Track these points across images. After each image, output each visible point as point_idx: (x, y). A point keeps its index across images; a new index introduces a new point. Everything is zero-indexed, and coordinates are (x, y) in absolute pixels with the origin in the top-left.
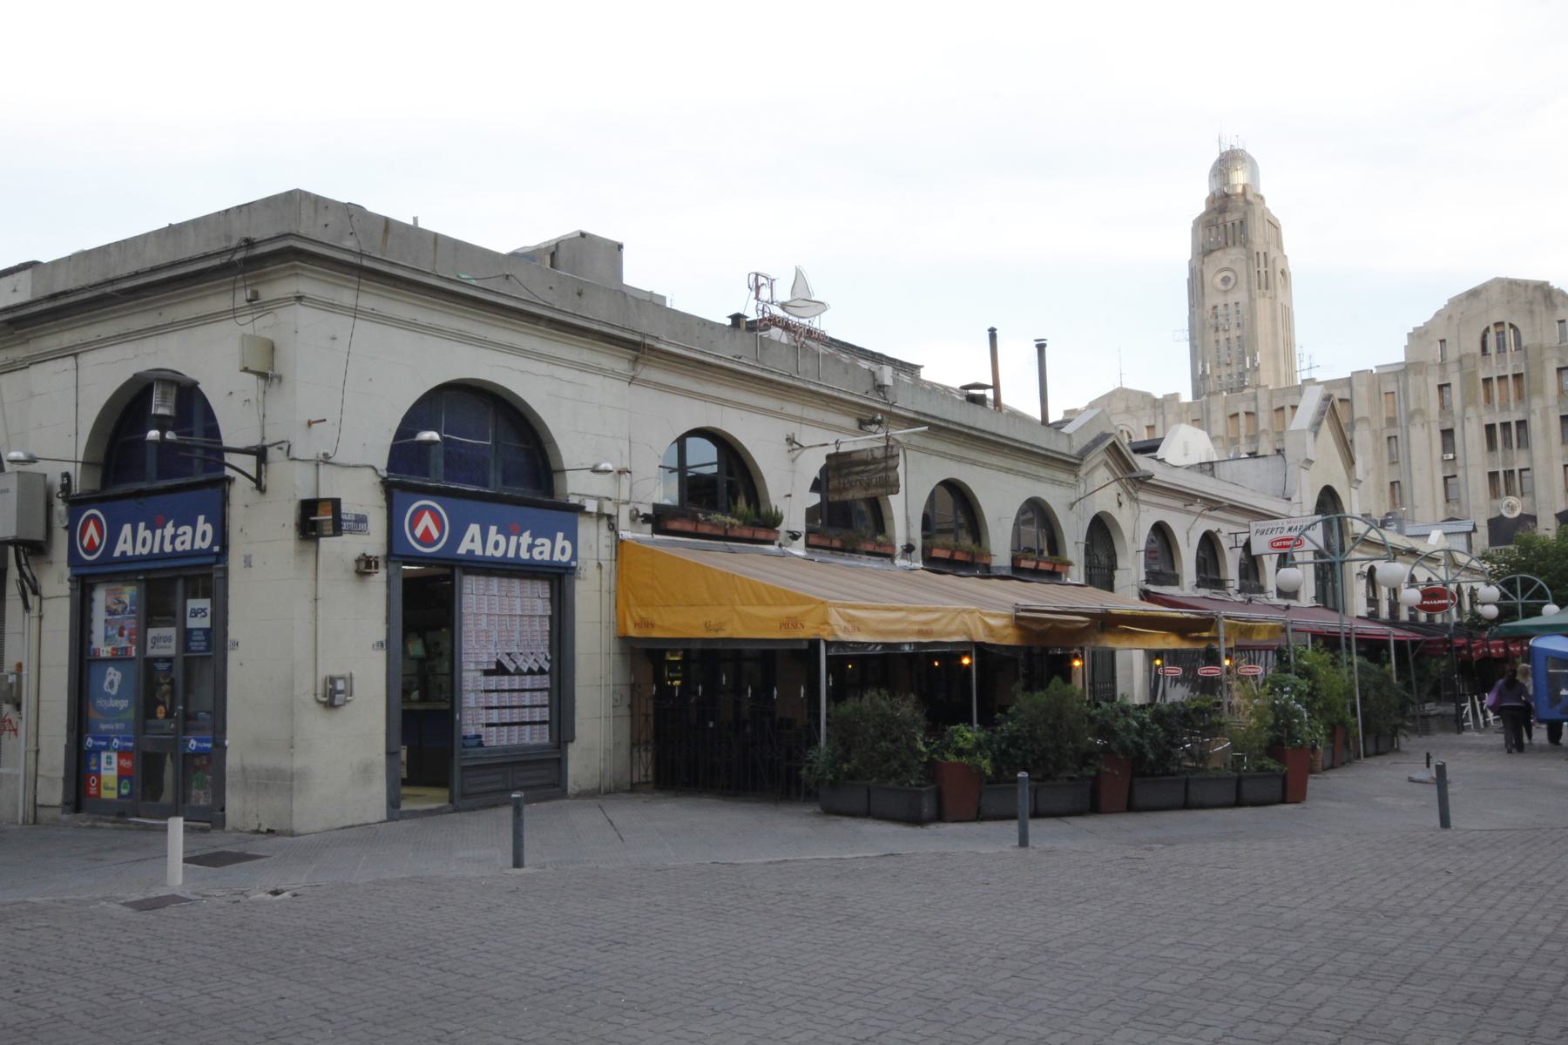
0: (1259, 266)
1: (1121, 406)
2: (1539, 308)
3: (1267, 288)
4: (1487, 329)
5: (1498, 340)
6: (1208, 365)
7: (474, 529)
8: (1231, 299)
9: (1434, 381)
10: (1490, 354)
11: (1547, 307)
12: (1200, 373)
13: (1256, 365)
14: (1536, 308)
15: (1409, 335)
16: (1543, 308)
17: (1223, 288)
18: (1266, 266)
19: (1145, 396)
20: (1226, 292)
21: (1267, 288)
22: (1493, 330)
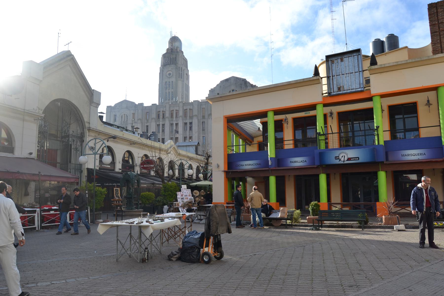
0: (179, 71)
3: (181, 78)
6: (163, 99)
8: (171, 80)
11: (245, 86)
13: (176, 101)
15: (210, 91)
16: (244, 87)
18: (181, 72)
19: (133, 103)
20: (169, 78)
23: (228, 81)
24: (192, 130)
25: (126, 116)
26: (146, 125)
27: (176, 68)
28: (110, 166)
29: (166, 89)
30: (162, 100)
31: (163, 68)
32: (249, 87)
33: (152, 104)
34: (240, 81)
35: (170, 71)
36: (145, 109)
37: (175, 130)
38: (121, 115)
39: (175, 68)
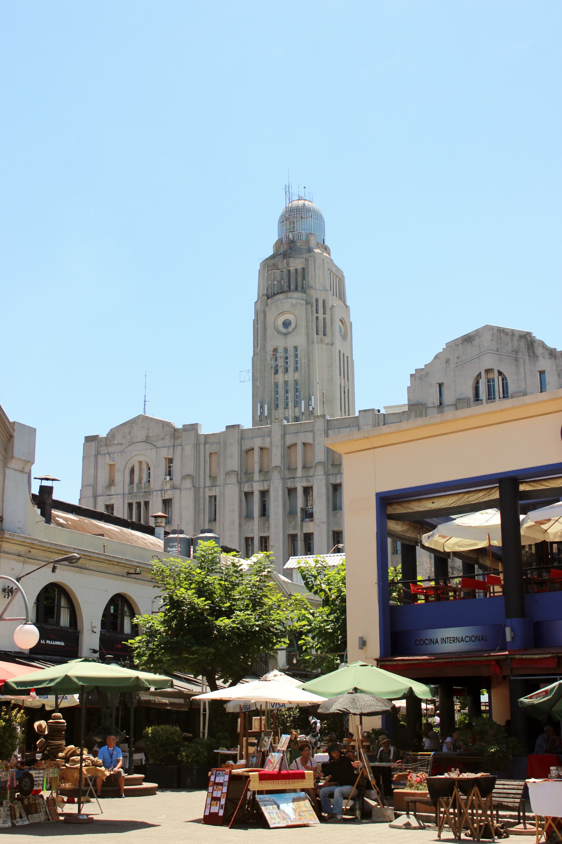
0: (317, 313)
1: (140, 435)
2: (524, 356)
3: (324, 335)
4: (480, 374)
5: (489, 386)
8: (291, 342)
10: (482, 400)
11: (529, 356)
12: (259, 414)
14: (520, 356)
15: (412, 375)
16: (527, 358)
17: (284, 330)
18: (324, 313)
19: (165, 425)
20: (286, 334)
23: (471, 342)
25: (144, 466)
26: (208, 493)
27: (307, 304)
28: (63, 644)
29: (276, 372)
30: (262, 407)
31: (267, 305)
32: (544, 358)
33: (227, 427)
34: (512, 341)
37: (302, 509)
38: (129, 466)
39: (304, 302)
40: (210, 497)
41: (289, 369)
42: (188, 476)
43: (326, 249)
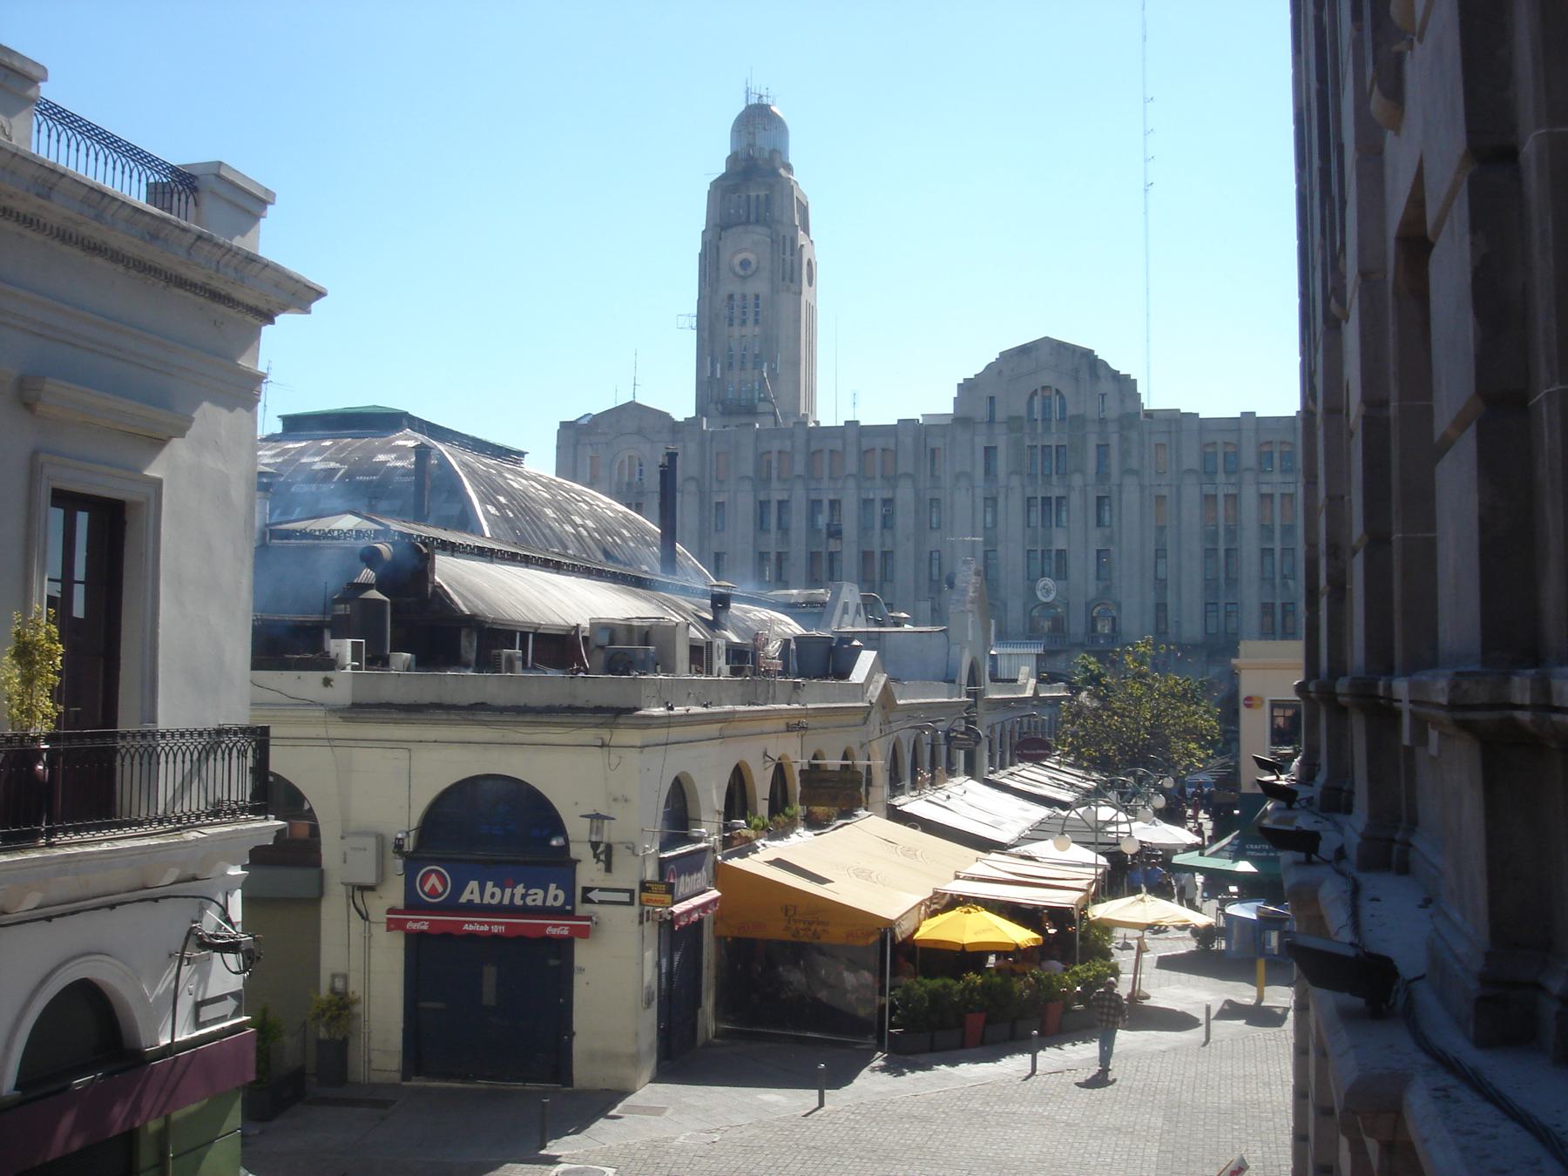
0: (784, 254)
6: (719, 366)
7: (474, 885)
8: (752, 288)
9: (981, 442)
18: (792, 255)
20: (744, 278)
21: (792, 281)
22: (1039, 391)
24: (891, 528)
27: (772, 242)
29: (731, 325)
35: (746, 250)
36: (711, 441)
39: (769, 240)
40: (717, 503)
41: (748, 322)
42: (692, 478)
43: (789, 168)
